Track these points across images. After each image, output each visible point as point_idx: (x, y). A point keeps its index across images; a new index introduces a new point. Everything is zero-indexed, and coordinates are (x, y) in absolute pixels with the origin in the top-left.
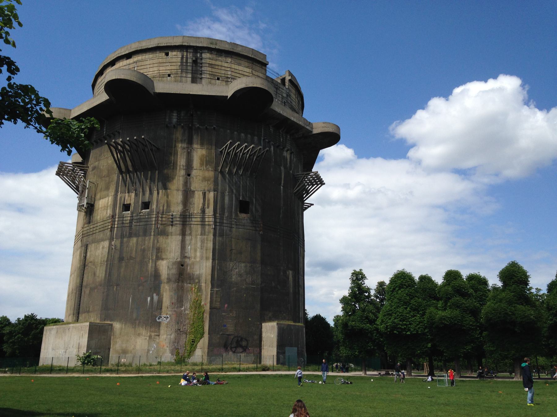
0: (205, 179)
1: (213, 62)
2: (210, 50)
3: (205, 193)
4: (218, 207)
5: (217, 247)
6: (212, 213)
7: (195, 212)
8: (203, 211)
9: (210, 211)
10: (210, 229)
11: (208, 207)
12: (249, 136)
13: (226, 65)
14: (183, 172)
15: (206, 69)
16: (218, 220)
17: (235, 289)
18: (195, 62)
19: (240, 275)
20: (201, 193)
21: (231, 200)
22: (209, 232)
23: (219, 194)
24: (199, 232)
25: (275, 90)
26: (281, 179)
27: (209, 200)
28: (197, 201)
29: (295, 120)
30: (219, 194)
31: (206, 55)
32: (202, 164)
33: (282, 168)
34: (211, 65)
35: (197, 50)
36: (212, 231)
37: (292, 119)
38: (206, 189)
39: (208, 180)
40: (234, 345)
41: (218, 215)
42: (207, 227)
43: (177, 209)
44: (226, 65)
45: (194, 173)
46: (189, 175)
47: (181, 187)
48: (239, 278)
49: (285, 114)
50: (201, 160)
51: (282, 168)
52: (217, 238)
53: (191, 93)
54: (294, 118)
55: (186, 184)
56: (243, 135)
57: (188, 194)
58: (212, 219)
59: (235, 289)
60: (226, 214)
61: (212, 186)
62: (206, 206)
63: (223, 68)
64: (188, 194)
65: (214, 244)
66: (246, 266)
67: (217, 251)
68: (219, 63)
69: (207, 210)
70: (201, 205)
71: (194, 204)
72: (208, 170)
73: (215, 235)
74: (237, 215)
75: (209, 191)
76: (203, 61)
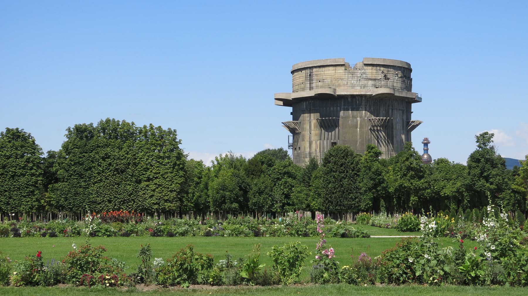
0: (316, 135)
1: (317, 73)
2: (316, 67)
9: (318, 150)
13: (322, 73)
14: (308, 132)
15: (315, 78)
18: (310, 75)
21: (327, 143)
26: (357, 125)
28: (314, 146)
29: (357, 93)
31: (314, 70)
33: (358, 119)
35: (311, 68)
37: (355, 93)
43: (308, 150)
44: (322, 73)
45: (312, 132)
49: (349, 93)
51: (358, 119)
55: (310, 138)
68: (319, 73)
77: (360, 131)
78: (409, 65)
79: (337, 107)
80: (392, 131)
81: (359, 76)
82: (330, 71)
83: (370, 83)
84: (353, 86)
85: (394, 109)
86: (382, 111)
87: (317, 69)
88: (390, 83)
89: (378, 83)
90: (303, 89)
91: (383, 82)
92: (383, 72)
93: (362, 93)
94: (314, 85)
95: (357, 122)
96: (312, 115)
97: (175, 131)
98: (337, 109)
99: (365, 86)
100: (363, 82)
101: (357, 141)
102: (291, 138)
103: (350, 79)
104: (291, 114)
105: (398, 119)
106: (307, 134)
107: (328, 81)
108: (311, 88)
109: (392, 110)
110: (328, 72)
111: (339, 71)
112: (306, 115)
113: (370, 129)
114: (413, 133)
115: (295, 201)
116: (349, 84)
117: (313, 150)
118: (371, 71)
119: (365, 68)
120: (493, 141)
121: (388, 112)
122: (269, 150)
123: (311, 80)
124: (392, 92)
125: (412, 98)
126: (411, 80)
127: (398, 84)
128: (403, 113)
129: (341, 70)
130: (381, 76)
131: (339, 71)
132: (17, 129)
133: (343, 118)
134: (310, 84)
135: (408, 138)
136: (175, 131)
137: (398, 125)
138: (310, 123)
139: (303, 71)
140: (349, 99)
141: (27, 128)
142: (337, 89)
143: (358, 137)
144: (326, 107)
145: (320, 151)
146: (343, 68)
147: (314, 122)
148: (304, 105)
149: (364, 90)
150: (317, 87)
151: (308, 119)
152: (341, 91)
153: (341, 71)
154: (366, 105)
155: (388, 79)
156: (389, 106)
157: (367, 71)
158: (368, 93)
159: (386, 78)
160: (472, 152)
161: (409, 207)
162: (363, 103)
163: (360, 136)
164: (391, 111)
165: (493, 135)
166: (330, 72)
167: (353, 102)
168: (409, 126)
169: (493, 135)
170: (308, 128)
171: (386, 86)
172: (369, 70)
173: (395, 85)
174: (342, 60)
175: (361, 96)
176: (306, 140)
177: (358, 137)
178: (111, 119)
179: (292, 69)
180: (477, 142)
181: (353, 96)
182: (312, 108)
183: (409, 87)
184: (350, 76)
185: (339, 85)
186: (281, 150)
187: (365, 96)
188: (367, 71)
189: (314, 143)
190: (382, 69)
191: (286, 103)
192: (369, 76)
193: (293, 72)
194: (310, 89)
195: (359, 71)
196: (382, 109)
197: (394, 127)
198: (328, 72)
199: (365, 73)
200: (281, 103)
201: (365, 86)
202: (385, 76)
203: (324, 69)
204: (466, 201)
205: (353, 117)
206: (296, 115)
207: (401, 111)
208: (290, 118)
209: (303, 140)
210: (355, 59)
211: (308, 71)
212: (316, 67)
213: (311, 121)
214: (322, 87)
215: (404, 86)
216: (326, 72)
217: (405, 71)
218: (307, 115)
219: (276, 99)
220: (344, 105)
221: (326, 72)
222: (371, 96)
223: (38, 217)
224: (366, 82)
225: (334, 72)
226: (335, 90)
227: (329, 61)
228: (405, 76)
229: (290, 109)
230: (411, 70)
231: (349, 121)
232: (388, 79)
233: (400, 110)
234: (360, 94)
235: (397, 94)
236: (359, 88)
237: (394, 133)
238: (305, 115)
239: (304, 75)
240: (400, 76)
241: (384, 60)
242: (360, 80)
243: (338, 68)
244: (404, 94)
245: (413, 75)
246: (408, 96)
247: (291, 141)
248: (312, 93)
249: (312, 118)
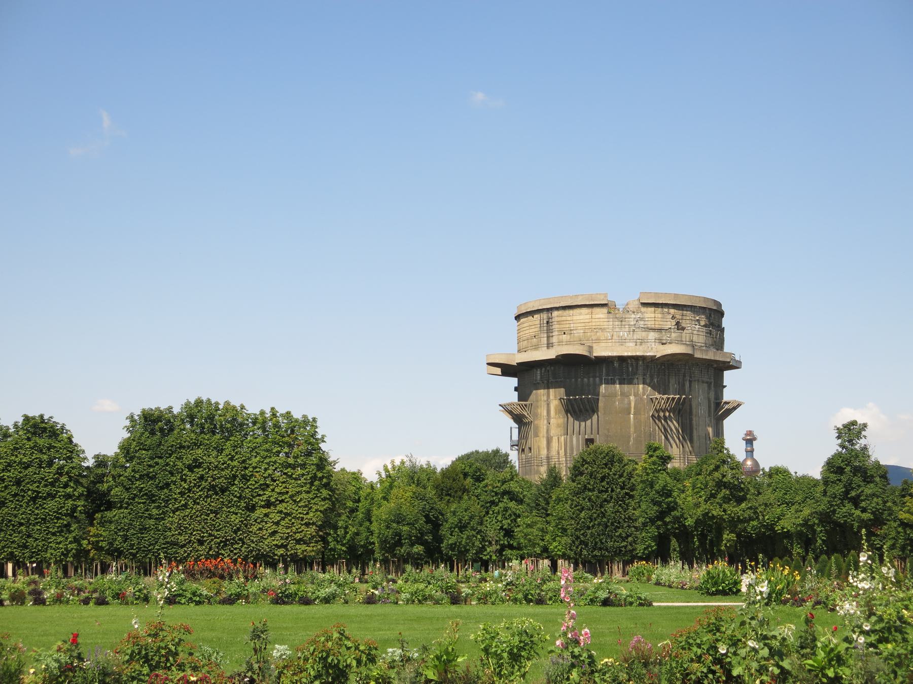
0: (558, 426)
2: (557, 309)
9: (562, 452)
12: (591, 379)
13: (569, 318)
14: (545, 422)
15: (555, 327)
18: (548, 322)
21: (578, 440)
26: (630, 407)
28: (555, 444)
29: (630, 354)
31: (555, 313)
33: (632, 398)
34: (559, 322)
35: (550, 310)
37: (626, 354)
43: (544, 452)
44: (569, 318)
45: (552, 421)
49: (615, 354)
51: (632, 398)
56: (586, 380)
68: (564, 318)
77: (634, 419)
78: (720, 305)
79: (594, 377)
80: (691, 420)
81: (632, 323)
82: (582, 315)
83: (652, 335)
84: (622, 341)
85: (693, 381)
86: (673, 383)
87: (560, 312)
88: (686, 335)
89: (665, 337)
90: (536, 347)
91: (673, 335)
92: (673, 317)
93: (638, 354)
94: (554, 340)
96: (552, 391)
97: (314, 420)
98: (594, 380)
99: (642, 342)
100: (640, 335)
101: (629, 437)
102: (515, 432)
103: (617, 330)
104: (516, 389)
105: (700, 397)
106: (542, 424)
107: (578, 333)
108: (549, 345)
109: (690, 382)
110: (578, 317)
111: (597, 316)
112: (541, 392)
113: (653, 416)
114: (727, 422)
115: (522, 541)
116: (615, 337)
117: (554, 452)
118: (653, 315)
119: (643, 309)
120: (865, 437)
121: (684, 385)
122: (477, 452)
123: (549, 331)
124: (690, 352)
125: (724, 362)
126: (722, 330)
127: (700, 338)
128: (709, 387)
129: (601, 313)
130: (670, 324)
131: (597, 316)
132: (42, 416)
133: (604, 396)
134: (548, 337)
135: (719, 432)
136: (314, 420)
137: (700, 409)
138: (548, 405)
139: (536, 316)
140: (616, 364)
141: (59, 415)
142: (595, 346)
143: (632, 429)
144: (575, 377)
145: (565, 454)
146: (605, 310)
147: (554, 403)
148: (538, 373)
149: (641, 348)
150: (560, 342)
152: (601, 351)
153: (602, 316)
154: (644, 375)
155: (683, 329)
156: (684, 376)
157: (646, 315)
159: (679, 326)
160: (829, 456)
161: (719, 550)
162: (640, 371)
163: (635, 428)
164: (687, 384)
165: (865, 425)
166: (582, 317)
167: (623, 369)
168: (720, 411)
169: (865, 425)
170: (545, 413)
171: (680, 342)
172: (649, 313)
173: (695, 338)
174: (602, 297)
175: (636, 358)
176: (541, 435)
177: (632, 429)
178: (205, 399)
179: (516, 312)
180: (838, 437)
181: (622, 359)
182: (551, 380)
183: (719, 344)
184: (617, 323)
185: (598, 340)
186: (496, 452)
187: (643, 358)
188: (646, 315)
189: (555, 440)
190: (672, 311)
191: (507, 370)
192: (651, 324)
193: (518, 318)
194: (548, 347)
195: (633, 316)
196: (672, 381)
197: (694, 411)
198: (578, 317)
199: (642, 319)
200: (498, 371)
201: (642, 342)
202: (678, 324)
203: (571, 312)
204: (820, 541)
205: (622, 394)
206: (523, 392)
207: (705, 385)
208: (514, 397)
209: (536, 435)
210: (625, 296)
211: (544, 316)
212: (557, 309)
213: (549, 402)
214: (569, 343)
215: (710, 341)
217: (713, 316)
218: (542, 391)
219: (489, 364)
220: (607, 375)
222: (653, 358)
223: (76, 570)
224: (644, 334)
225: (588, 316)
226: (591, 348)
227: (580, 298)
228: (712, 324)
229: (514, 381)
230: (722, 314)
231: (615, 402)
232: (683, 329)
233: (703, 382)
235: (698, 355)
236: (632, 345)
237: (694, 422)
238: (539, 391)
239: (538, 322)
240: (703, 323)
241: (676, 295)
242: (634, 331)
243: (596, 310)
244: (711, 355)
245: (725, 322)
246: (717, 358)
247: (515, 437)
248: (551, 354)
249: (552, 397)
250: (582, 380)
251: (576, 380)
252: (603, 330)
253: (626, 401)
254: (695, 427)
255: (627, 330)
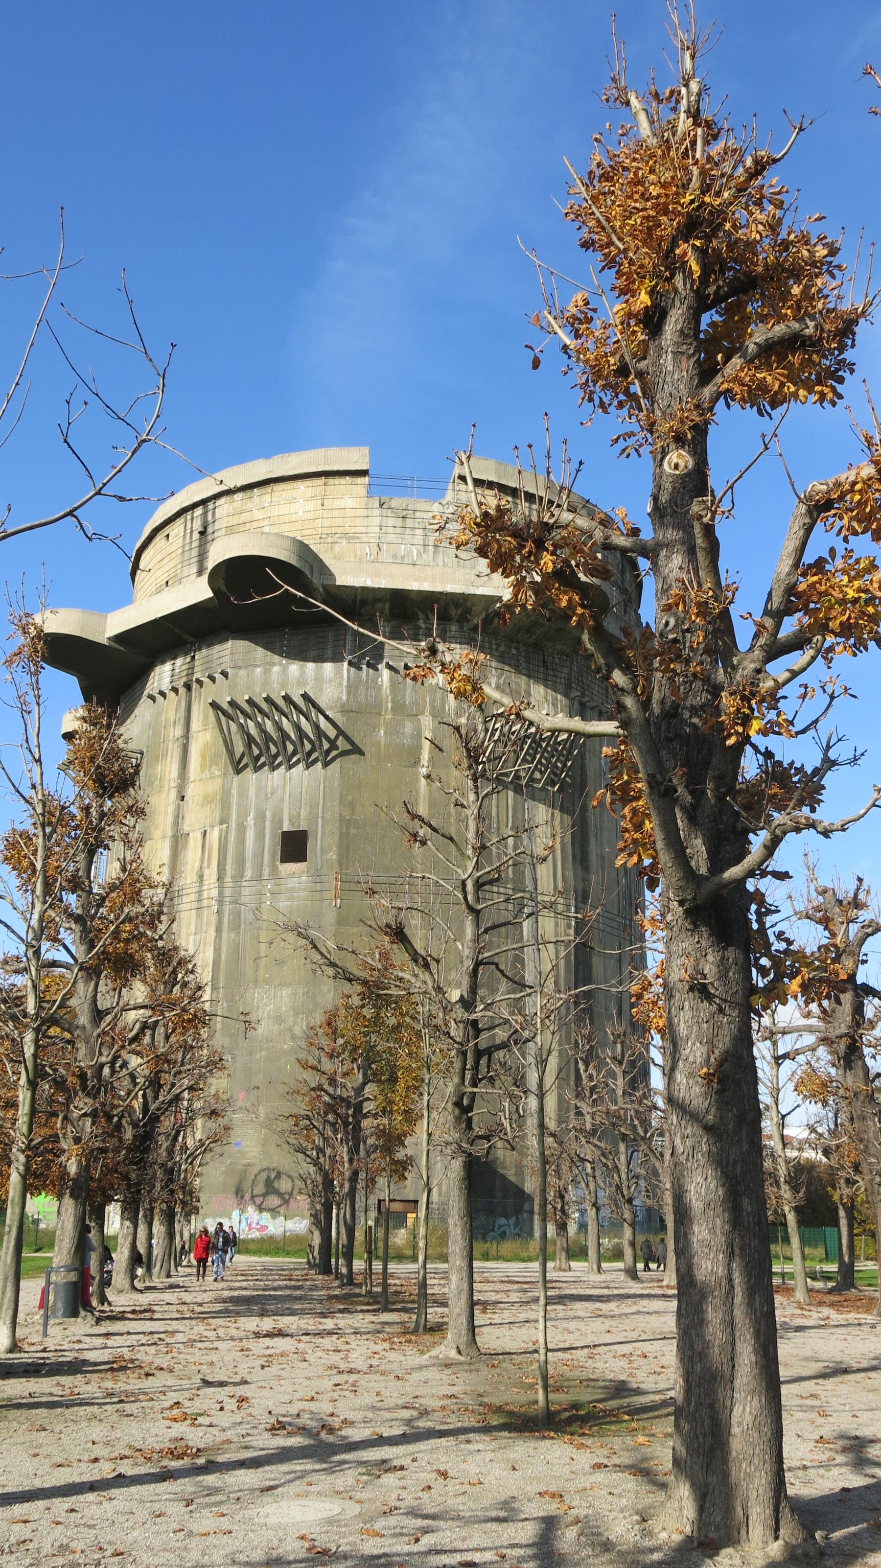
0: (207, 800)
1: (235, 520)
3: (205, 832)
4: (229, 861)
5: (223, 957)
6: (215, 877)
7: (188, 881)
8: (201, 878)
9: (211, 875)
10: (210, 916)
11: (208, 867)
14: (173, 795)
16: (228, 892)
17: (264, 1053)
19: (279, 1019)
20: (199, 835)
22: (208, 924)
23: (233, 825)
24: (193, 927)
25: (399, 522)
27: (210, 848)
29: (426, 587)
30: (233, 825)
32: (203, 767)
36: (214, 919)
37: (414, 586)
38: (208, 822)
39: (211, 802)
40: (260, 1189)
41: (228, 879)
42: (205, 912)
45: (192, 791)
46: (183, 797)
47: (169, 833)
48: (276, 1027)
50: (203, 757)
52: (225, 936)
53: (160, 615)
54: (418, 579)
55: (178, 818)
57: (178, 841)
58: (215, 893)
59: (264, 1053)
60: (248, 874)
61: (217, 815)
62: (206, 863)
63: (255, 525)
64: (178, 841)
65: (217, 950)
66: (295, 994)
67: (223, 966)
68: (246, 517)
69: (206, 872)
70: (198, 864)
71: (186, 863)
72: (212, 777)
73: (219, 930)
74: (274, 870)
75: (212, 827)
76: (217, 525)
93: (450, 588)
95: (418, 735)
103: (391, 538)
111: (337, 504)
116: (384, 556)
131: (337, 504)
145: (220, 878)
151: (179, 731)
153: (349, 502)
158: (479, 591)
184: (391, 522)
205: (399, 708)
216: (275, 511)
221: (275, 511)
231: (375, 728)
234: (438, 588)
250: (285, 669)
251: (267, 672)
252: (351, 538)
253: (408, 728)
254: (592, 828)
255: (419, 540)
